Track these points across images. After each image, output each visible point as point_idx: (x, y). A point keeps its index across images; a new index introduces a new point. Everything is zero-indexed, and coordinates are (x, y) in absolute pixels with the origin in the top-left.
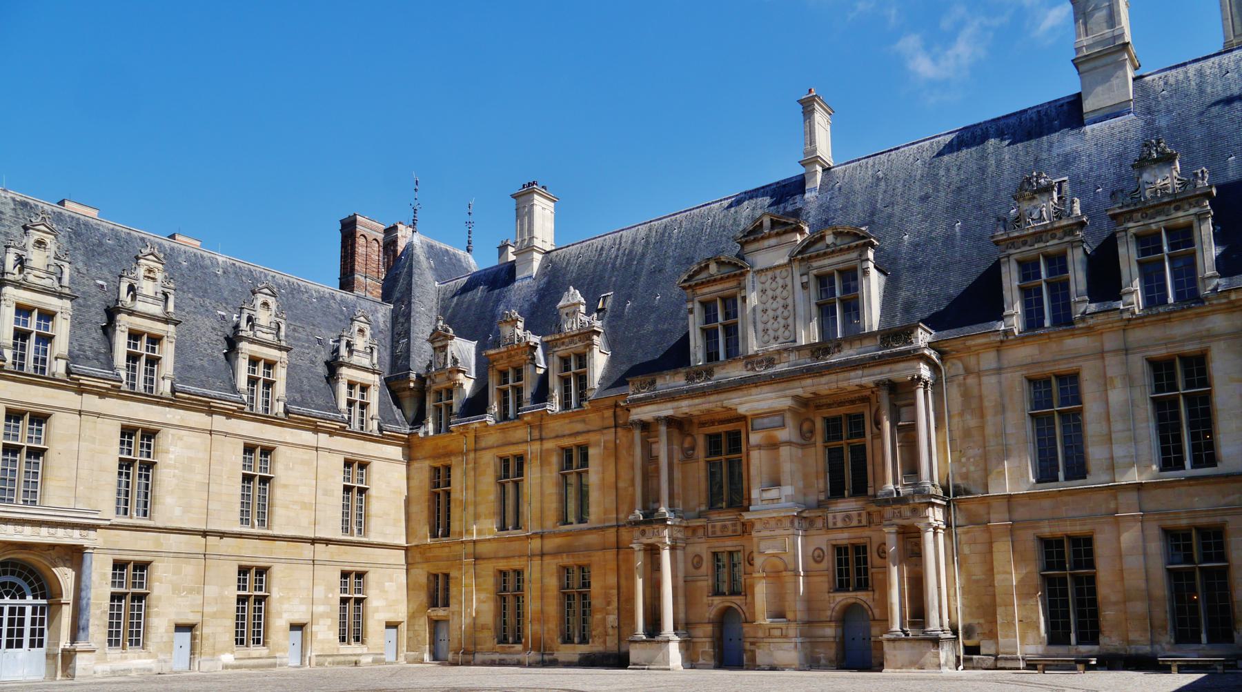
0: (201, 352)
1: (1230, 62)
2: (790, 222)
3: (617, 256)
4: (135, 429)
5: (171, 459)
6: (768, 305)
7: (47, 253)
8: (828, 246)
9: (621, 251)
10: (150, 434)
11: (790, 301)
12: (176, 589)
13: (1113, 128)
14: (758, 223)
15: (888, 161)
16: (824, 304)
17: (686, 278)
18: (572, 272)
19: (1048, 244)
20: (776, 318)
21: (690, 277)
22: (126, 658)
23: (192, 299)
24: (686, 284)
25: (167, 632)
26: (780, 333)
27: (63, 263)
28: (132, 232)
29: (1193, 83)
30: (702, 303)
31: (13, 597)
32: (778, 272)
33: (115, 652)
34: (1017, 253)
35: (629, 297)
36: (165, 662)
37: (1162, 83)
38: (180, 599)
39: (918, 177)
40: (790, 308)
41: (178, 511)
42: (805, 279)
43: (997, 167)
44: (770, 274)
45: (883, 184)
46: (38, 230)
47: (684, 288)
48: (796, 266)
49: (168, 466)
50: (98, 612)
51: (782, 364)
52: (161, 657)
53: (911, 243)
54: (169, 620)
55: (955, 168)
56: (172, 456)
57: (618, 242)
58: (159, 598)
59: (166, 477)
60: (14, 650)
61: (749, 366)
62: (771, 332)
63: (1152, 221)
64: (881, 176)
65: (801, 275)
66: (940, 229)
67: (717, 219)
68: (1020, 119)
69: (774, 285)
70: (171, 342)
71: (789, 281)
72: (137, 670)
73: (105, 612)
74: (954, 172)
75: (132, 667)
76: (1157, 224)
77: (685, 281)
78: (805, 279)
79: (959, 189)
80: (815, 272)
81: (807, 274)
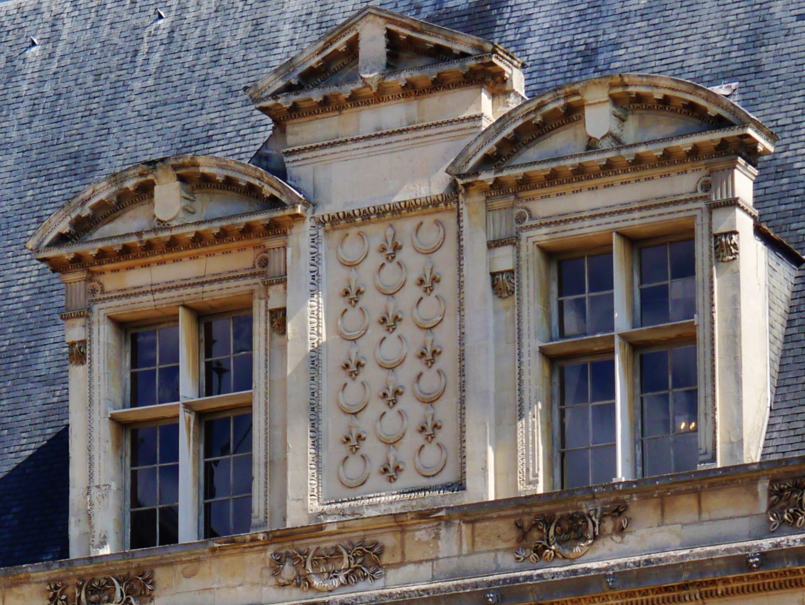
2: (457, 48)
6: (366, 349)
8: (591, 145)
11: (445, 337)
14: (340, 45)
16: (647, 344)
17: (64, 227)
20: (392, 397)
24: (66, 252)
26: (405, 452)
30: (122, 326)
32: (406, 226)
40: (447, 362)
42: (504, 259)
44: (377, 233)
47: (57, 266)
51: (410, 568)
61: (288, 571)
62: (372, 448)
65: (493, 245)
67: (190, 16)
69: (390, 275)
71: (445, 262)
77: (62, 239)
78: (504, 259)
80: (542, 235)
81: (512, 241)
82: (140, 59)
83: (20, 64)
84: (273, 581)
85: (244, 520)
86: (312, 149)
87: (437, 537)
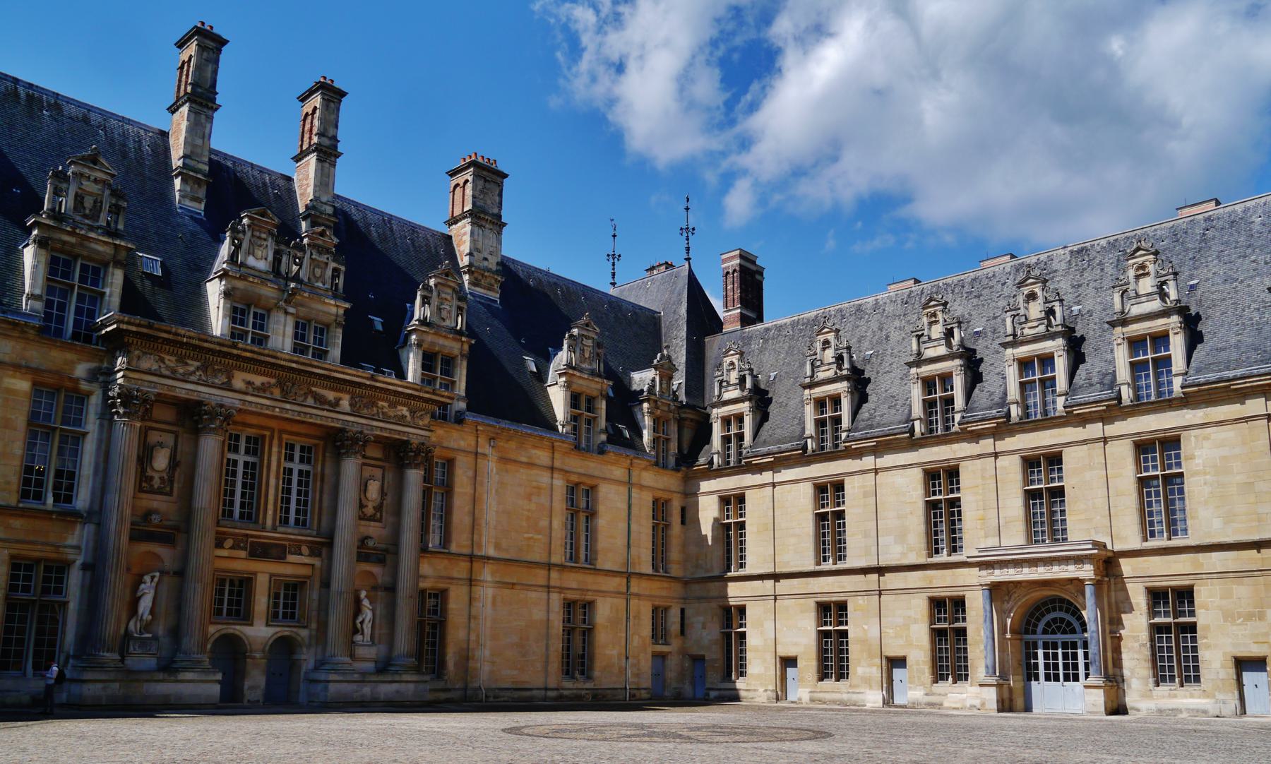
0: (1243, 324)
4: (1152, 442)
5: (1197, 465)
7: (1039, 301)
10: (1170, 443)
12: (1229, 616)
22: (1175, 696)
23: (1254, 261)
25: (1223, 667)
27: (1053, 303)
28: (1196, 217)
31: (1064, 632)
33: (1164, 688)
36: (1224, 703)
38: (1235, 628)
41: (1217, 523)
46: (1027, 285)
49: (1196, 473)
50: (1137, 645)
52: (1220, 696)
54: (1225, 654)
56: (1197, 461)
58: (1207, 628)
59: (1196, 487)
60: (1072, 683)
70: (1177, 333)
72: (1188, 710)
73: (1144, 645)
75: (1180, 706)
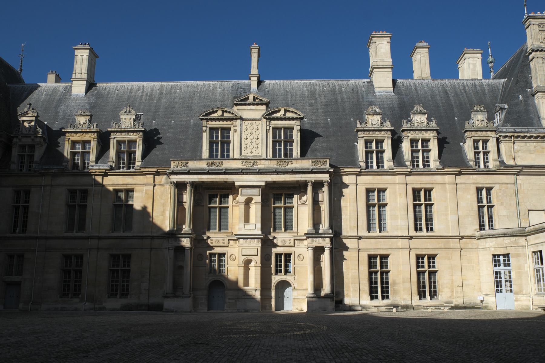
1: (424, 84)
2: (263, 100)
3: (142, 96)
9: (144, 94)
13: (387, 97)
14: (247, 97)
15: (290, 85)
18: (113, 97)
19: (378, 136)
21: (206, 115)
24: (205, 118)
29: (413, 88)
32: (254, 122)
34: (412, 135)
35: (154, 118)
37: (401, 84)
39: (306, 95)
43: (342, 100)
44: (250, 122)
45: (289, 95)
47: (202, 119)
48: (264, 120)
51: (261, 165)
53: (309, 123)
55: (323, 96)
57: (141, 88)
61: (244, 164)
63: (417, 135)
64: (288, 91)
66: (321, 120)
67: (202, 90)
68: (348, 83)
74: (322, 97)
76: (419, 136)
77: (203, 116)
79: (326, 105)
80: (273, 126)
82: (196, 94)
83: (176, 92)
84: (241, 165)
85: (228, 156)
86: (241, 109)
87: (265, 162)
